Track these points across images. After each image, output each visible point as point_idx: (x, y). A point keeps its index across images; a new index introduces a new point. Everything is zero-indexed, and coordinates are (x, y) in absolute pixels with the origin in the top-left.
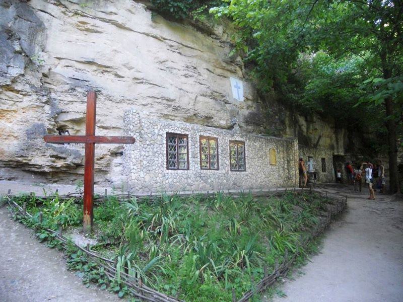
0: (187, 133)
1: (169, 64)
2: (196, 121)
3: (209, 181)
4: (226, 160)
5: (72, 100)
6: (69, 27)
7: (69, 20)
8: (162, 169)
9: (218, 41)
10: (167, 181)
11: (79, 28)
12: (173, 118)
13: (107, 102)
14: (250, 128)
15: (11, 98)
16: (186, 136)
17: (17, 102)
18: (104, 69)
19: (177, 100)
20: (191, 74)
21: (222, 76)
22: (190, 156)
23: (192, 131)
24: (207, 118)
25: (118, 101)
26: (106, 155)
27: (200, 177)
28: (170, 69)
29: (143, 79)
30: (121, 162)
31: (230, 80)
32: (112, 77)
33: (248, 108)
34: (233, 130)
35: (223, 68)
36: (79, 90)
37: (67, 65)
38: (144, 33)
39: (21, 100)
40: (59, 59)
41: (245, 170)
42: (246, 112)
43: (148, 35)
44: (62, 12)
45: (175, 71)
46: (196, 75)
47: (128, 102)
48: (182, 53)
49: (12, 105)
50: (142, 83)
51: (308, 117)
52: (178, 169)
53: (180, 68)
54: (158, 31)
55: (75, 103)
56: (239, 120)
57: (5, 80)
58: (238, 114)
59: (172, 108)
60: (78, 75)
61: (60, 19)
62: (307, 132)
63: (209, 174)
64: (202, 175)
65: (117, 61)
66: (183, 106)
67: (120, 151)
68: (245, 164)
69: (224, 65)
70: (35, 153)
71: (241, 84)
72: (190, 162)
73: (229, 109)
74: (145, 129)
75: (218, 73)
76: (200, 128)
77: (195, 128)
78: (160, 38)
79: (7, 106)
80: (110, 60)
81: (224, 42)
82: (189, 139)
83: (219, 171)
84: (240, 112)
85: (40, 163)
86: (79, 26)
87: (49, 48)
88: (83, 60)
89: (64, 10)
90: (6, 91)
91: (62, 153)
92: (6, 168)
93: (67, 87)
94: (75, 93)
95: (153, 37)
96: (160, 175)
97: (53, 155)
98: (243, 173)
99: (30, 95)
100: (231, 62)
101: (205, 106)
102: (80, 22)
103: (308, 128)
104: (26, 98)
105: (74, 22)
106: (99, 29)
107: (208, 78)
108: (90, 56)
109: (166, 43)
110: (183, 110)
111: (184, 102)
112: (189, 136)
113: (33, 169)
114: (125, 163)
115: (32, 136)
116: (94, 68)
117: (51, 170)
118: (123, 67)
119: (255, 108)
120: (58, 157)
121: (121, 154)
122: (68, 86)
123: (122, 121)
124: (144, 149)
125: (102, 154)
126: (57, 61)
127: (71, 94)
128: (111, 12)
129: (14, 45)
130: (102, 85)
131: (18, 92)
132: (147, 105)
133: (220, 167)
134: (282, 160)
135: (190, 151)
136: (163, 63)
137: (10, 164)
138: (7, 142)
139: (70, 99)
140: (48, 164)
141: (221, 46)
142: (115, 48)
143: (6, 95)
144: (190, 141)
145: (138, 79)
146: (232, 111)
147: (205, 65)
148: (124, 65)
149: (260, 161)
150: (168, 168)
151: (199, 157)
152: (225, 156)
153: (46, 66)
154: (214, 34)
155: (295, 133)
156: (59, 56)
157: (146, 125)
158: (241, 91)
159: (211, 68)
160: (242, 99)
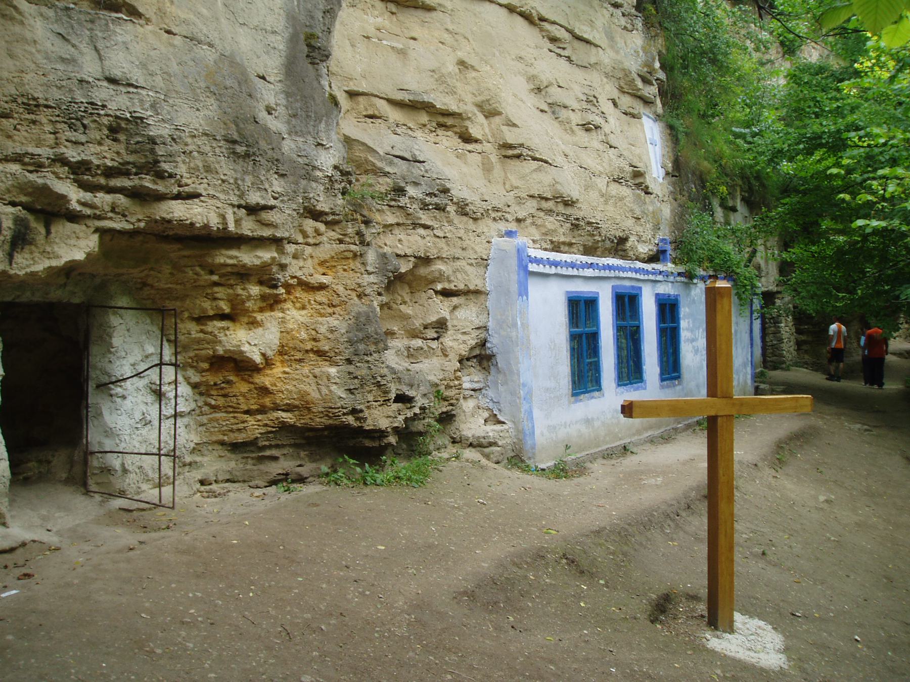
13: (457, 219)
18: (441, 120)
21: (630, 114)
29: (522, 145)
31: (642, 125)
32: (456, 141)
37: (370, 112)
45: (564, 114)
47: (493, 215)
48: (573, 58)
50: (518, 156)
53: (575, 105)
55: (396, 231)
88: (399, 96)
94: (403, 201)
95: (522, 15)
108: (417, 84)
109: (542, 30)
113: (368, 443)
116: (424, 118)
122: (388, 180)
127: (393, 203)
142: (460, 54)
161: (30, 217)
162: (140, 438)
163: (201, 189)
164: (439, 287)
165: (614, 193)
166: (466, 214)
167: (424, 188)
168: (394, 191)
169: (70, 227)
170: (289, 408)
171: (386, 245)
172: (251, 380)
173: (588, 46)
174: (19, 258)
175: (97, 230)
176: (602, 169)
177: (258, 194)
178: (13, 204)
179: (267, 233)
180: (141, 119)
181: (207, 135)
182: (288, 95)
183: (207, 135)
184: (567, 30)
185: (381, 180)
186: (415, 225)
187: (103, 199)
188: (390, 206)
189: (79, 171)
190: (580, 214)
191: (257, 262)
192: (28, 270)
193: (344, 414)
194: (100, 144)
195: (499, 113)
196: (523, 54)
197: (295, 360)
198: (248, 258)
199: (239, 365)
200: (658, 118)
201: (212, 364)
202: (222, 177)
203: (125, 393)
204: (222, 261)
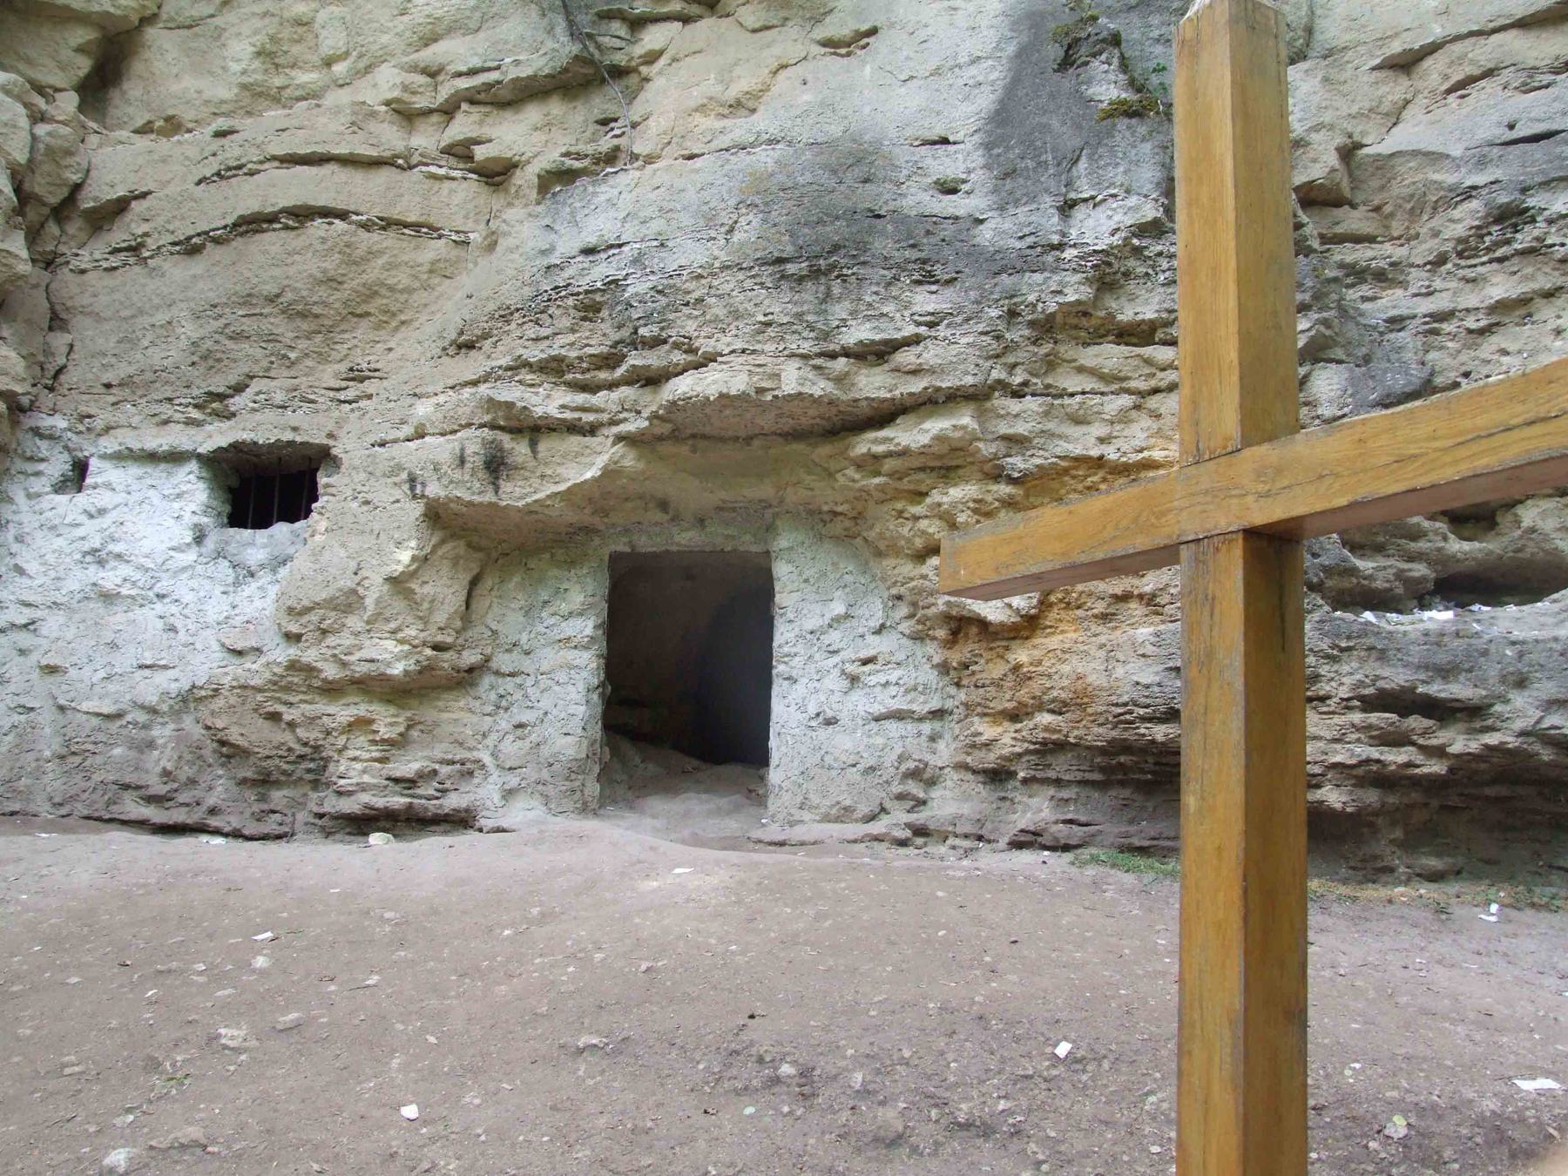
5: (1514, 293)
17: (1156, 391)
40: (1405, 64)
49: (1123, 418)
55: (1545, 312)
57: (1054, 282)
90: (1086, 344)
91: (1446, 672)
92: (1113, 793)
94: (1524, 239)
97: (1382, 693)
126: (1395, 89)
127: (1499, 253)
129: (1089, 82)
139: (1500, 287)
143: (1081, 370)
153: (1314, 137)
156: (1396, 47)
161: (506, 440)
163: (720, 347)
168: (1498, 221)
169: (575, 441)
170: (1059, 708)
171: (1505, 352)
174: (506, 487)
175: (620, 438)
177: (868, 325)
178: (482, 426)
179: (917, 386)
180: (615, 282)
181: (728, 267)
182: (988, 146)
183: (728, 267)
187: (599, 399)
188: (1500, 260)
189: (554, 368)
191: (925, 439)
192: (529, 500)
193: (1144, 719)
194: (573, 331)
197: (1095, 616)
198: (913, 435)
201: (955, 633)
202: (762, 318)
203: (794, 674)
204: (864, 450)
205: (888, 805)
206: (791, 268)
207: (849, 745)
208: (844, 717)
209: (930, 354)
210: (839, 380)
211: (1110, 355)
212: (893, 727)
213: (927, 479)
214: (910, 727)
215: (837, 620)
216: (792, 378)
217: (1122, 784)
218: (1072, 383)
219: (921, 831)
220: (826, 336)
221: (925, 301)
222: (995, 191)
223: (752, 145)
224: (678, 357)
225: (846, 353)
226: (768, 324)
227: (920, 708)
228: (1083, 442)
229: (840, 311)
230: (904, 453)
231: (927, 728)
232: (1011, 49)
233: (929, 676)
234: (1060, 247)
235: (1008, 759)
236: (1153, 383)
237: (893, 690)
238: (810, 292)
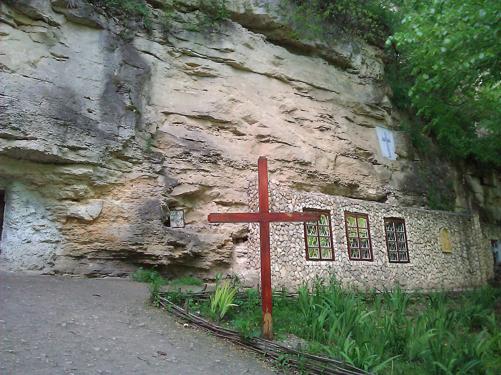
0: (328, 208)
1: (299, 114)
2: (336, 191)
3: (362, 277)
4: (381, 247)
6: (175, 71)
7: (176, 62)
8: (301, 259)
9: (356, 76)
10: (308, 277)
11: (188, 71)
12: (308, 188)
14: (409, 198)
15: (119, 168)
16: (327, 212)
17: (126, 172)
18: (221, 125)
19: (313, 162)
20: (327, 125)
21: (365, 125)
22: (334, 241)
23: (334, 205)
24: (350, 186)
25: (241, 167)
26: (229, 241)
27: (350, 271)
28: (300, 121)
30: (246, 251)
31: (376, 131)
32: (231, 135)
33: (402, 170)
34: (387, 202)
35: (367, 115)
36: (195, 154)
38: (265, 74)
39: (130, 169)
40: (167, 114)
41: (409, 262)
42: (400, 176)
43: (269, 76)
44: (168, 52)
45: (306, 123)
46: (333, 127)
47: (252, 168)
49: (120, 177)
50: (268, 141)
51: (486, 181)
52: (321, 260)
54: (282, 69)
55: (189, 172)
56: (392, 187)
58: (390, 179)
59: (308, 176)
60: (191, 134)
61: (165, 62)
62: (485, 202)
63: (361, 266)
64: (353, 269)
65: (236, 114)
66: (321, 170)
67: (244, 235)
68: (408, 252)
69: (368, 109)
70: (150, 239)
71: (390, 135)
72: (336, 249)
73: (379, 172)
74: (277, 204)
75: (360, 122)
76: (345, 201)
77: (338, 200)
78: (286, 79)
79: (115, 178)
80: (227, 112)
81: (364, 77)
82: (332, 217)
83: (374, 263)
84: (393, 176)
85: (157, 253)
86: (188, 69)
87: (154, 100)
89: (170, 49)
91: (181, 239)
93: (179, 151)
94: (189, 158)
95: (276, 78)
96: (299, 269)
98: (406, 265)
99: (141, 163)
100: (377, 104)
101: (348, 171)
102: (188, 64)
103: (486, 195)
104: (136, 168)
105: (181, 64)
106: (212, 72)
107: (348, 130)
110: (320, 177)
111: (322, 166)
112: (332, 213)
113: (148, 261)
114: (252, 251)
115: (147, 217)
116: (210, 124)
117: (169, 262)
118: (243, 121)
119: (411, 169)
120: (177, 246)
121: (245, 239)
122: (181, 149)
123: (245, 194)
124: (277, 232)
125: (223, 240)
126: (164, 117)
128: (227, 49)
130: (220, 147)
131: (127, 159)
132: (275, 171)
133: (375, 257)
134: (459, 245)
135: (333, 233)
136: (291, 113)
137: (120, 255)
138: (115, 225)
139: (183, 166)
140: (167, 253)
141: (361, 84)
142: (232, 96)
143: (114, 164)
144: (333, 220)
145: (263, 137)
146: (382, 175)
147: (343, 112)
148: (245, 119)
149: (428, 248)
150: (308, 259)
151: (346, 243)
152: (380, 240)
153: (153, 124)
154: (350, 67)
155: (468, 204)
156: (166, 110)
157: (278, 199)
158: (392, 145)
159: (351, 116)
160: (394, 157)
162: (24, 248)
164: (217, 200)
165: (342, 161)
166: (232, 167)
167: (202, 153)
172: (86, 228)
173: (325, 91)
176: (331, 149)
179: (83, 160)
182: (101, 105)
184: (307, 83)
185: (178, 149)
186: (199, 170)
190: (313, 170)
193: (130, 245)
195: (257, 122)
196: (275, 96)
199: (81, 220)
200: (391, 128)
201: (67, 220)
203: (18, 227)
205: (45, 265)
206: (59, 122)
207: (36, 249)
208: (33, 240)
209: (88, 153)
210: (64, 153)
211: (119, 162)
212: (46, 244)
213: (74, 181)
214: (50, 245)
215: (32, 214)
216: (55, 151)
217: (116, 259)
218: (113, 167)
219: (56, 272)
220: (64, 141)
221: (88, 140)
222: (102, 117)
223: (44, 81)
224: (22, 135)
225: (68, 147)
226: (51, 134)
227: (54, 240)
228: (112, 180)
229: (69, 136)
230: (74, 174)
231: (54, 245)
232: (105, 81)
233: (55, 231)
234: (117, 136)
235: (86, 253)
236: (126, 170)
237: (48, 234)
238: (62, 129)
